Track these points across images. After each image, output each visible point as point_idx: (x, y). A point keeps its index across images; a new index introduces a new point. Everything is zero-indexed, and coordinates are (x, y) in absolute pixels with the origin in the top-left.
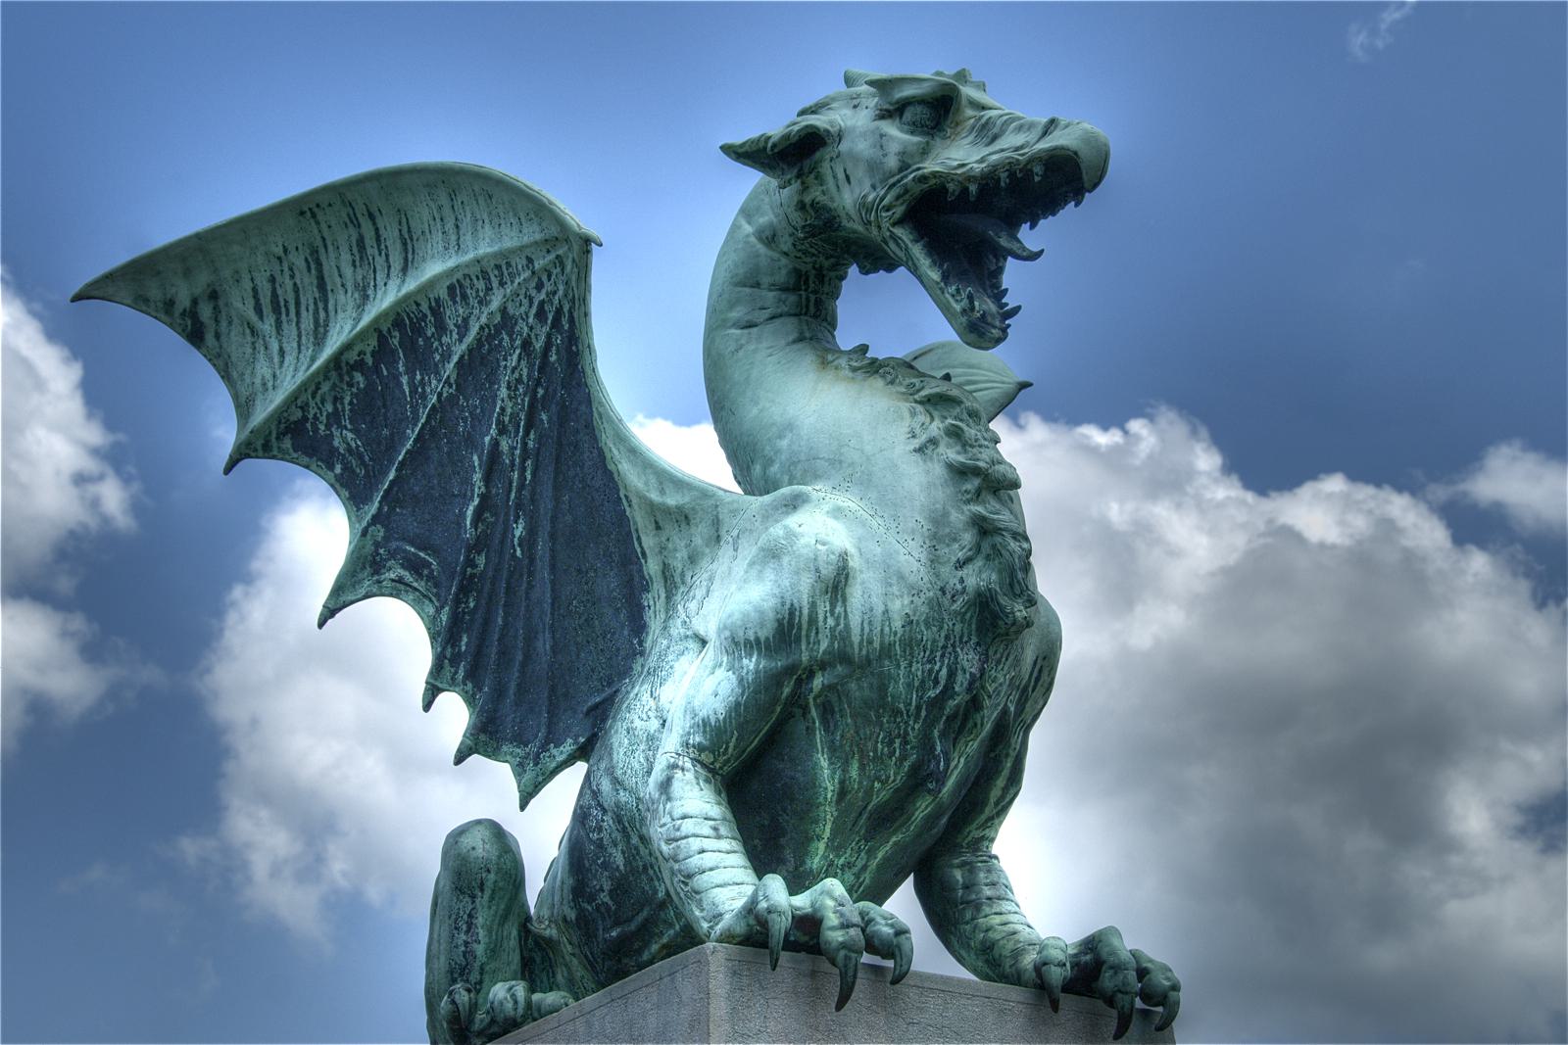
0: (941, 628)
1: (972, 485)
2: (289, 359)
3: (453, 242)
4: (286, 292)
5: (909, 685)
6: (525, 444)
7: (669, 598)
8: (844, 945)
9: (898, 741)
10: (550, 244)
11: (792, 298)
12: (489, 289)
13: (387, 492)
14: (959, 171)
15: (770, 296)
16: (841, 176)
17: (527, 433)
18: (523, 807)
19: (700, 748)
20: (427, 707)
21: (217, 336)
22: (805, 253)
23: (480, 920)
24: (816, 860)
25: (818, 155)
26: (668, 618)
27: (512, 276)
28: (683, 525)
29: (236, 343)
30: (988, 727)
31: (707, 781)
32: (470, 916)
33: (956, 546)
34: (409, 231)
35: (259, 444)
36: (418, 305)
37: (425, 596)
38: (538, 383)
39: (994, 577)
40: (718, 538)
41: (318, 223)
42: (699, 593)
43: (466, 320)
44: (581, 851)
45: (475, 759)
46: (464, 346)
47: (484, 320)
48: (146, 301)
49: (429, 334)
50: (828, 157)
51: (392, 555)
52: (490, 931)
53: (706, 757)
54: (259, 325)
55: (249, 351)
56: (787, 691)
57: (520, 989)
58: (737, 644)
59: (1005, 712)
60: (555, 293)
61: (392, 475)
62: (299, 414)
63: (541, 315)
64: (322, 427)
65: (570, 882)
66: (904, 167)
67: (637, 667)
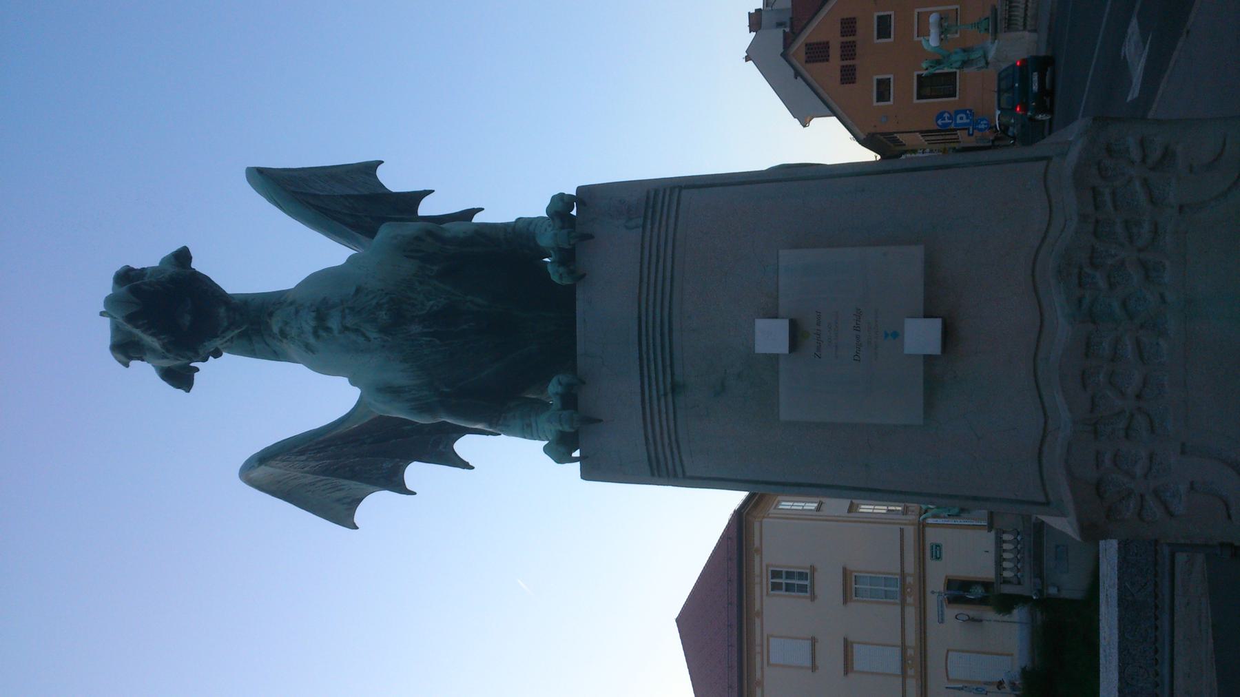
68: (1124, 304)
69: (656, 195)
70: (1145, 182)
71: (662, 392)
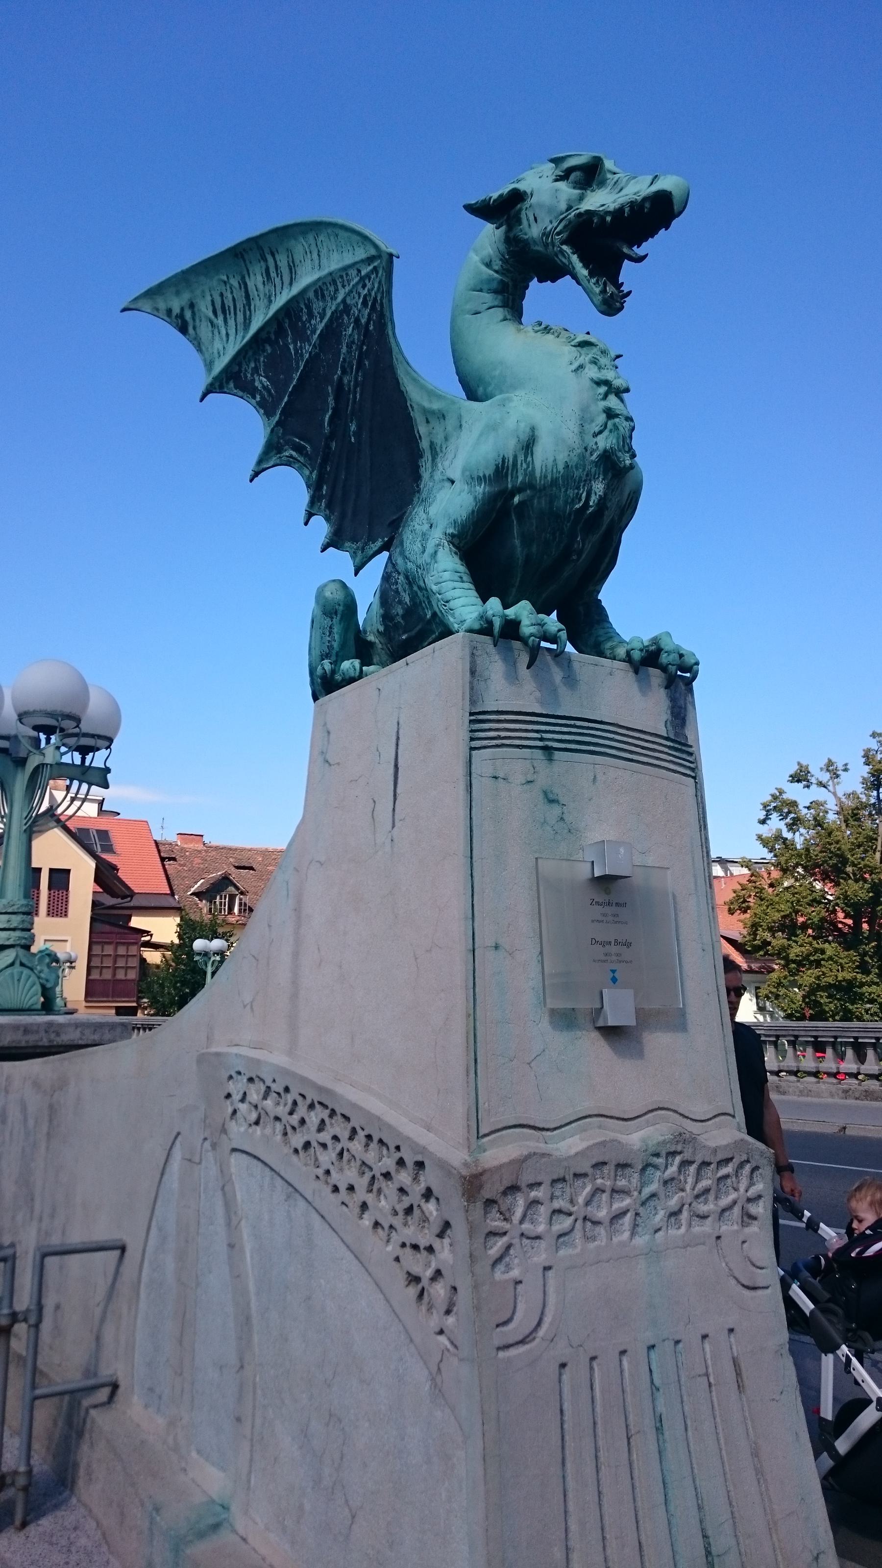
0: (584, 470)
1: (603, 389)
2: (232, 338)
3: (317, 262)
4: (229, 302)
5: (566, 502)
6: (356, 379)
7: (434, 459)
8: (532, 635)
9: (557, 534)
10: (370, 260)
11: (500, 297)
12: (337, 290)
13: (283, 408)
14: (601, 209)
15: (488, 298)
16: (532, 218)
17: (357, 372)
18: (356, 574)
19: (453, 536)
20: (306, 524)
21: (194, 328)
22: (508, 270)
23: (335, 630)
24: (511, 598)
25: (519, 206)
26: (433, 471)
27: (349, 281)
28: (442, 420)
29: (204, 331)
30: (604, 527)
31: (456, 553)
32: (331, 628)
33: (594, 424)
34: (293, 262)
35: (217, 385)
36: (298, 303)
37: (305, 465)
38: (363, 343)
39: (614, 441)
40: (461, 426)
41: (245, 261)
42: (450, 456)
43: (324, 310)
44: (386, 596)
45: (331, 549)
46: (323, 324)
47: (333, 308)
48: (157, 310)
49: (304, 319)
50: (524, 208)
51: (287, 443)
52: (340, 636)
53: (456, 541)
54: (215, 320)
55: (210, 335)
56: (499, 504)
57: (357, 663)
58: (472, 478)
59: (612, 520)
60: (372, 289)
61: (286, 399)
62: (236, 368)
63: (365, 303)
64: (249, 375)
65: (382, 611)
66: (569, 208)
67: (416, 499)
68: (653, 1195)
69: (691, 754)
70: (735, 1202)
71: (545, 736)
